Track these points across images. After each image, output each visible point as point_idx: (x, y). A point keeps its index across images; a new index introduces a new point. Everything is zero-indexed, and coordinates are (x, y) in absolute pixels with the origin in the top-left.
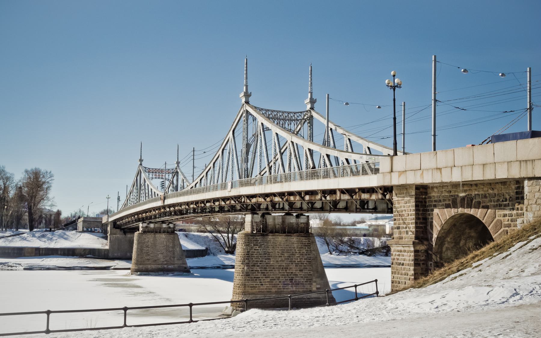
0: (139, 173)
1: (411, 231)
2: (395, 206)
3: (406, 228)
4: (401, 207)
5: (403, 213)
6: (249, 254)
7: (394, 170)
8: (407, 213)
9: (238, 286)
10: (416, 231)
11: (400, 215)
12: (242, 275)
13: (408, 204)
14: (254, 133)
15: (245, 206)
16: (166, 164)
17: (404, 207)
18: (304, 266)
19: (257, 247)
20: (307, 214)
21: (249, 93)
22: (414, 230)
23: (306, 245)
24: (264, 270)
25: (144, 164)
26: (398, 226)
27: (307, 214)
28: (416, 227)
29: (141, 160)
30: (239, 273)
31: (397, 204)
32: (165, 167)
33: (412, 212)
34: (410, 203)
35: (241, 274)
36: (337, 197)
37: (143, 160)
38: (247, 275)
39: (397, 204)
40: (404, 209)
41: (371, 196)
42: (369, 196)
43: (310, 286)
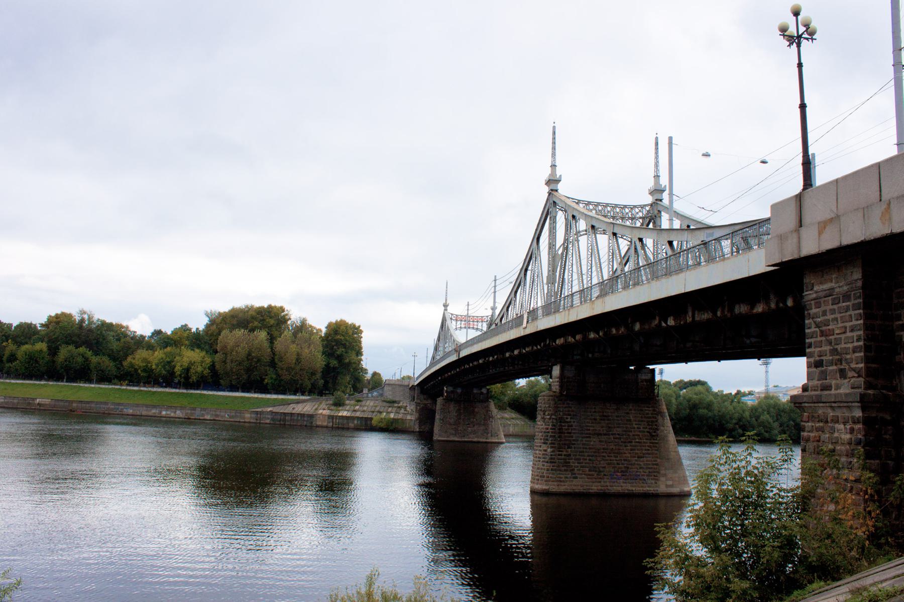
0: (444, 321)
1: (854, 370)
2: (809, 314)
3: (840, 361)
4: (824, 313)
5: (830, 327)
6: (554, 429)
7: (807, 219)
8: (840, 325)
9: (537, 478)
10: (867, 369)
11: (822, 332)
12: (543, 461)
13: (844, 304)
16: (468, 305)
17: (833, 311)
19: (569, 417)
20: (651, 367)
21: (558, 177)
22: (862, 365)
23: (650, 415)
24: (579, 455)
25: (450, 309)
26: (818, 358)
27: (651, 367)
28: (867, 360)
30: (539, 458)
31: (813, 307)
33: (854, 322)
34: (849, 300)
35: (541, 460)
36: (688, 318)
37: (447, 306)
38: (551, 462)
39: (813, 307)
40: (833, 316)
41: (752, 308)
42: (749, 308)
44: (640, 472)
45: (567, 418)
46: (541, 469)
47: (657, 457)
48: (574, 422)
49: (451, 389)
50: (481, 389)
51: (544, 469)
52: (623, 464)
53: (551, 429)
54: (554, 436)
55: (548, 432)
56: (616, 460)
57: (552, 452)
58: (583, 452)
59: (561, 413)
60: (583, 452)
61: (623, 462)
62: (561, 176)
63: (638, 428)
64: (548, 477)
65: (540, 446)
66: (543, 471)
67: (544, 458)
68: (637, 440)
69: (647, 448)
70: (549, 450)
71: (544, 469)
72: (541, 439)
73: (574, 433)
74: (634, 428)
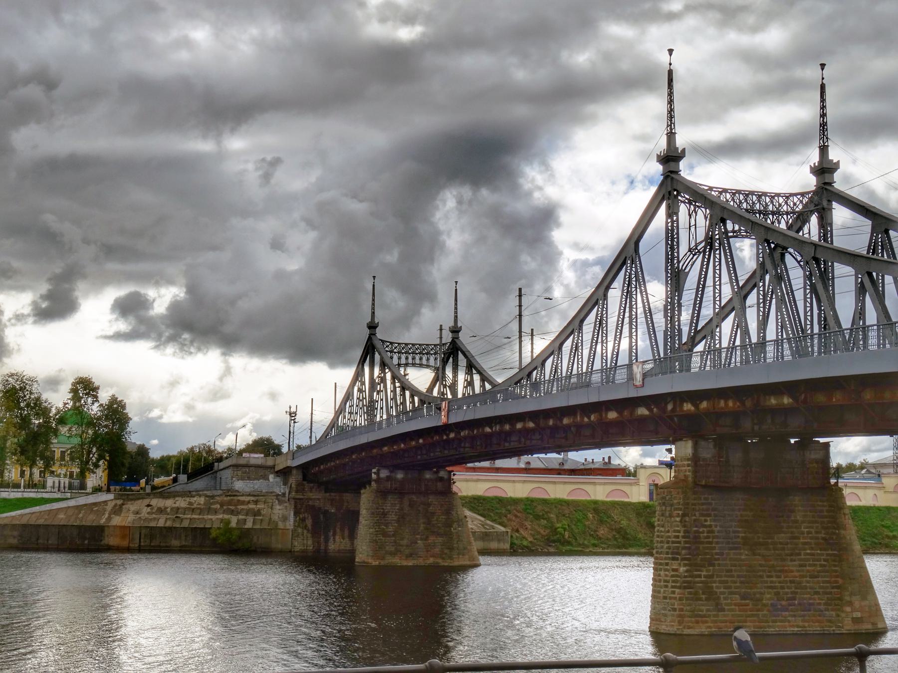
6: (688, 537)
12: (673, 587)
14: (693, 244)
15: (676, 419)
18: (821, 565)
19: (708, 519)
20: (822, 440)
23: (825, 514)
24: (726, 576)
27: (822, 440)
29: (372, 327)
32: (441, 338)
35: (670, 585)
43: (838, 616)
44: (814, 599)
45: (706, 521)
46: (671, 598)
47: (837, 577)
48: (716, 526)
49: (384, 473)
50: (437, 472)
51: (675, 598)
52: (788, 588)
53: (683, 537)
54: (689, 548)
55: (679, 542)
56: (780, 582)
57: (687, 571)
58: (731, 571)
59: (697, 513)
60: (731, 571)
61: (789, 584)
62: (684, 150)
63: (809, 533)
64: (681, 610)
65: (667, 564)
66: (673, 601)
67: (673, 581)
68: (808, 551)
69: (823, 563)
70: (682, 569)
71: (675, 598)
72: (667, 553)
73: (717, 543)
74: (803, 533)
